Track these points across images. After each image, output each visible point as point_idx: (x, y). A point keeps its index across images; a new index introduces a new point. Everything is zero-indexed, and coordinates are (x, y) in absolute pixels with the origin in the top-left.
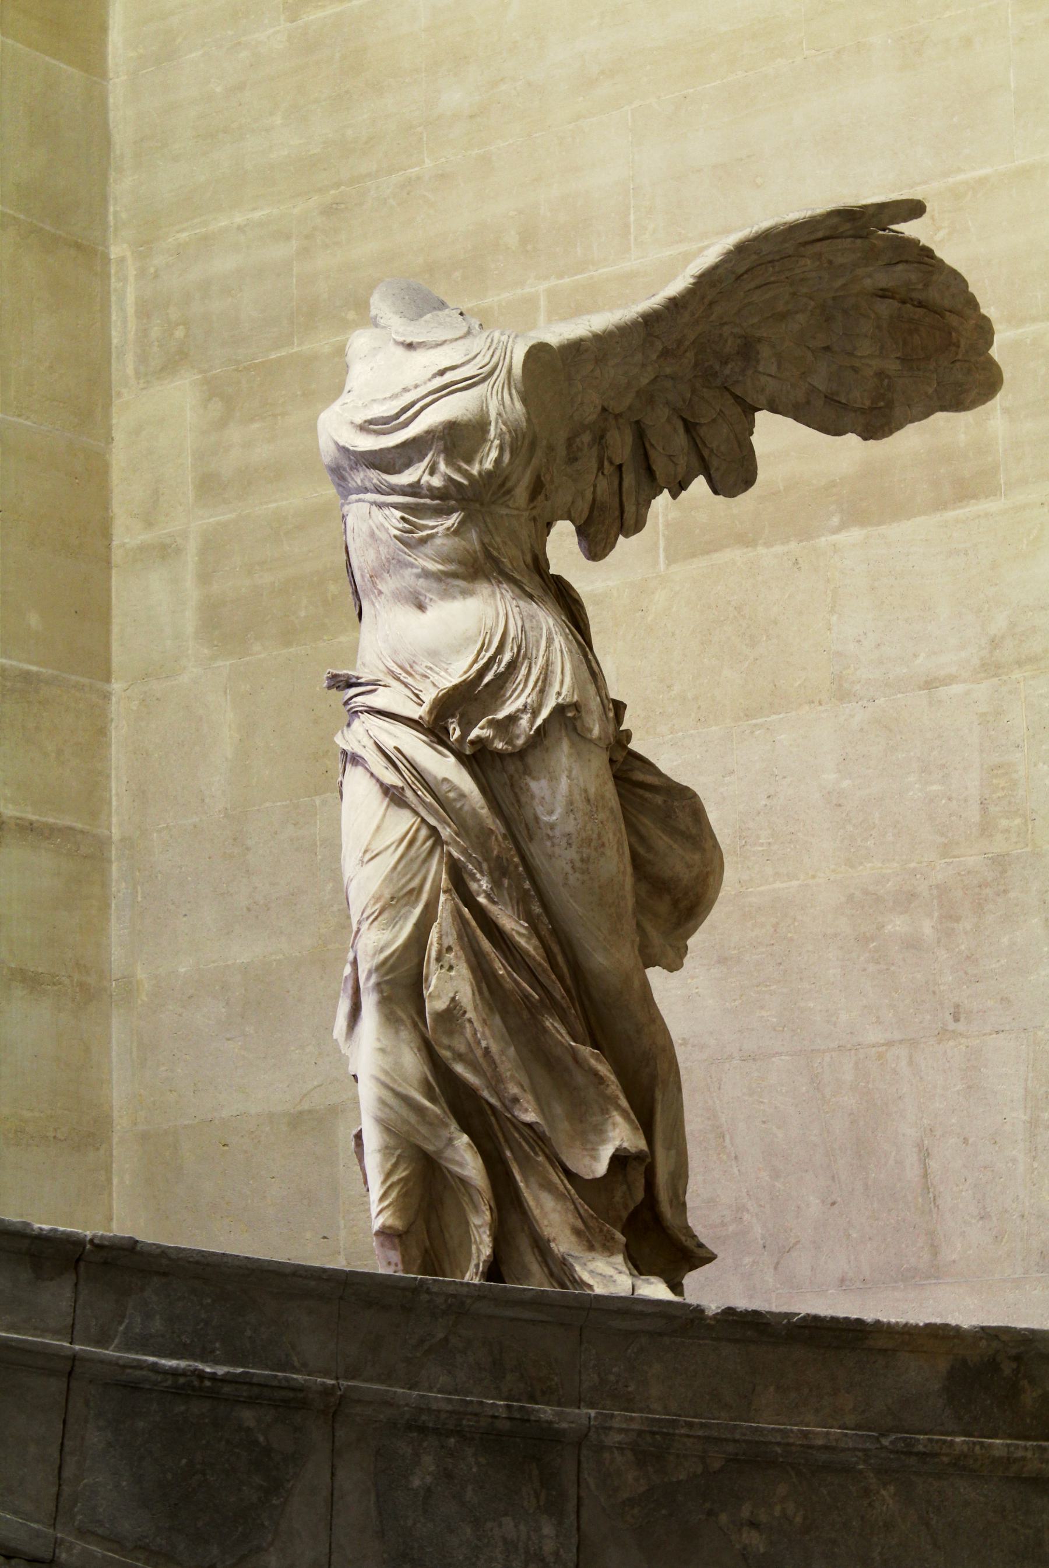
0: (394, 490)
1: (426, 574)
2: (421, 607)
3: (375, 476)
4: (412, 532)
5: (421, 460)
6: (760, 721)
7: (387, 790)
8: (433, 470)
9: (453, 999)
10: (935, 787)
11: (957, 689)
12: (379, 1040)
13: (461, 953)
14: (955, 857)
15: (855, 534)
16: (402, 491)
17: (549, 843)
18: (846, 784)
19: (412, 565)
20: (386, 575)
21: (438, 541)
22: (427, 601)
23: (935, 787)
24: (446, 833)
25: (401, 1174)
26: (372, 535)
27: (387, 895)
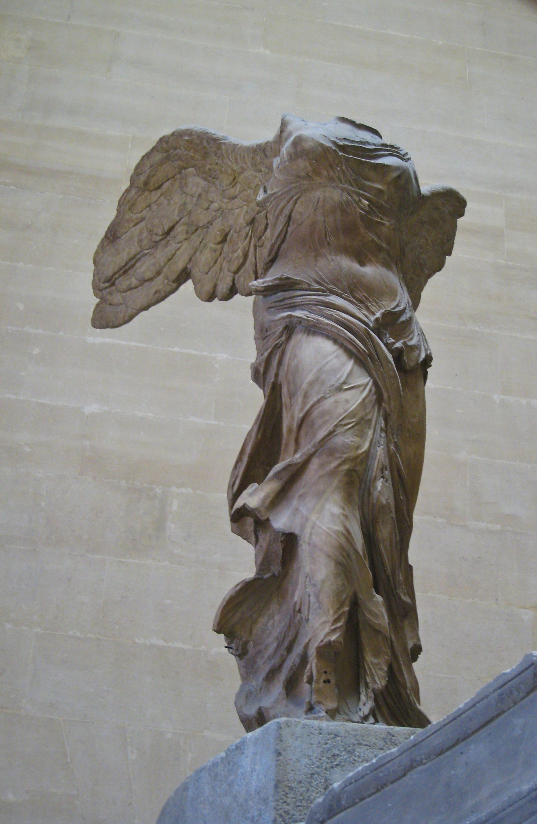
9: (387, 500)
12: (344, 509)
13: (389, 473)
17: (408, 435)
24: (385, 396)
25: (346, 609)
27: (361, 414)
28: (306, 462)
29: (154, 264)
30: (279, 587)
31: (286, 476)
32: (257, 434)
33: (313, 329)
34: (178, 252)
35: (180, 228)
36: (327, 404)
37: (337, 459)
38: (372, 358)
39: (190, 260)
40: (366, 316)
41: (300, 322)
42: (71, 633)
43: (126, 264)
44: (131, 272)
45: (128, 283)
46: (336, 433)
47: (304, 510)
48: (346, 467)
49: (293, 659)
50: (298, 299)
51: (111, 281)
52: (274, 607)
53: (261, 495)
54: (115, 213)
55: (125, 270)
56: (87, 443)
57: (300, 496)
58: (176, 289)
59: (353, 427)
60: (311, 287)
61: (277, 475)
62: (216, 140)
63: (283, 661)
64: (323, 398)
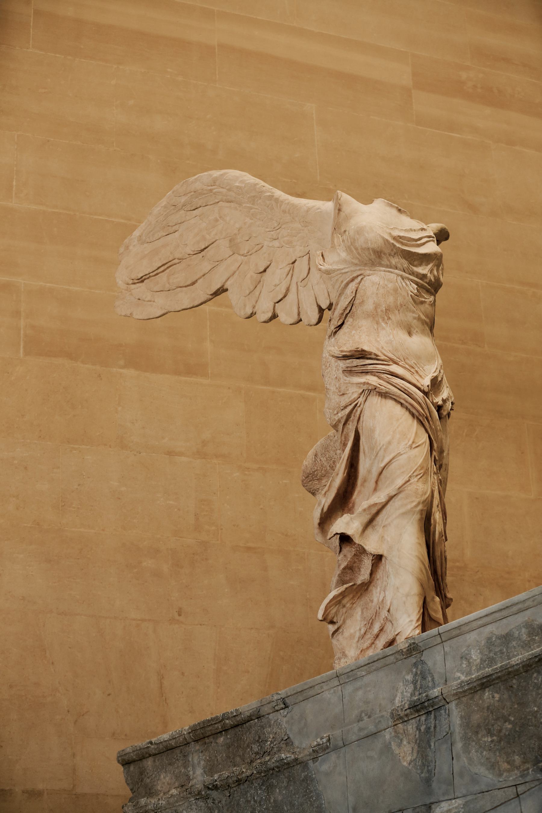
0: (413, 273)
1: (419, 319)
2: (410, 334)
3: (405, 264)
4: (418, 296)
5: (427, 265)
6: (76, 446)
7: (413, 415)
8: (431, 271)
10: (171, 502)
11: (184, 459)
12: (418, 538)
14: (181, 537)
15: (131, 372)
16: (418, 275)
18: (123, 489)
19: (414, 312)
20: (397, 312)
21: (427, 306)
22: (415, 331)
23: (171, 502)
24: (435, 445)
26: (396, 290)
30: (367, 589)
31: (374, 510)
32: (344, 473)
33: (384, 395)
36: (402, 459)
37: (412, 502)
38: (427, 418)
41: (375, 389)
46: (410, 482)
48: (420, 507)
57: (384, 526)
59: (421, 477)
60: (378, 358)
64: (399, 454)
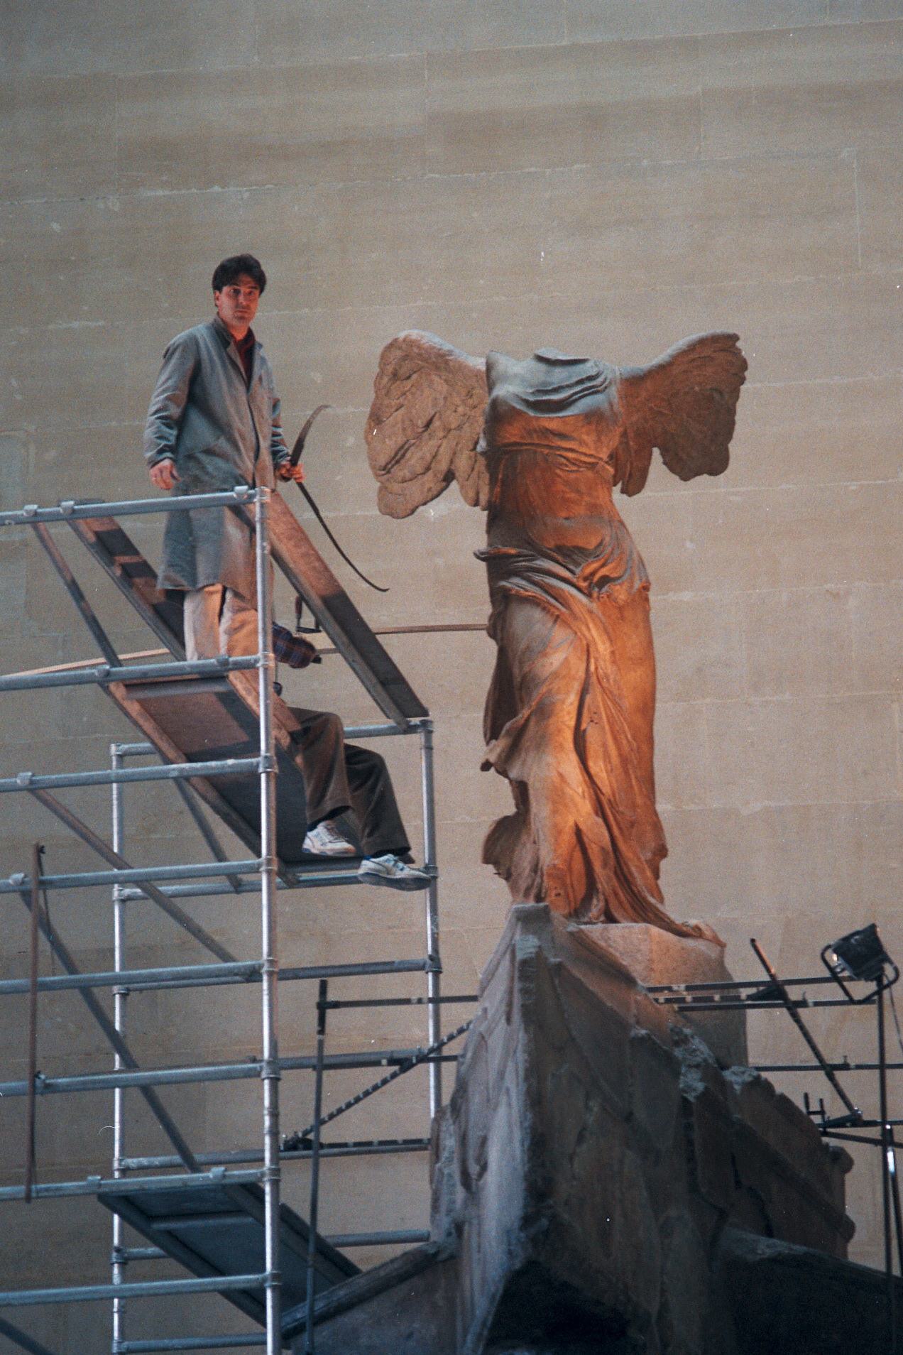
28: (528, 720)
29: (422, 458)
34: (442, 450)
35: (437, 423)
39: (452, 462)
40: (572, 572)
42: (458, 820)
43: (396, 454)
44: (402, 461)
45: (401, 474)
47: (529, 761)
49: (538, 880)
50: (512, 567)
51: (386, 469)
52: (524, 838)
53: (498, 750)
54: (373, 396)
55: (398, 457)
56: (440, 561)
58: (447, 487)
61: (508, 731)
62: (442, 356)
63: (533, 881)
